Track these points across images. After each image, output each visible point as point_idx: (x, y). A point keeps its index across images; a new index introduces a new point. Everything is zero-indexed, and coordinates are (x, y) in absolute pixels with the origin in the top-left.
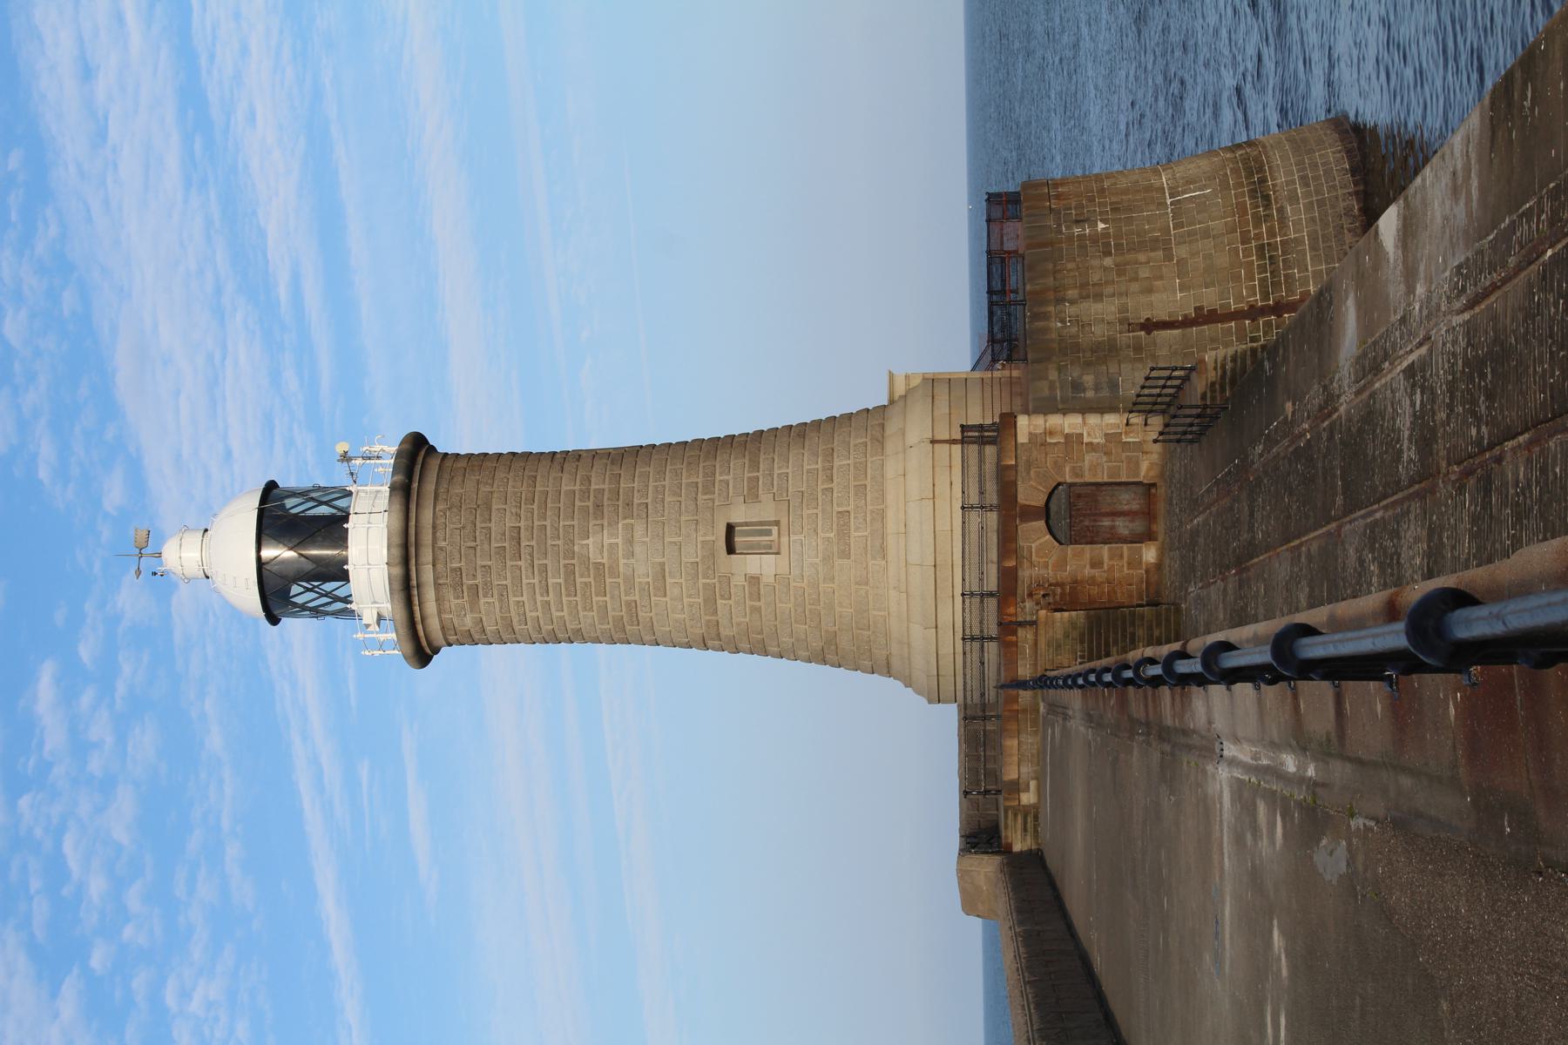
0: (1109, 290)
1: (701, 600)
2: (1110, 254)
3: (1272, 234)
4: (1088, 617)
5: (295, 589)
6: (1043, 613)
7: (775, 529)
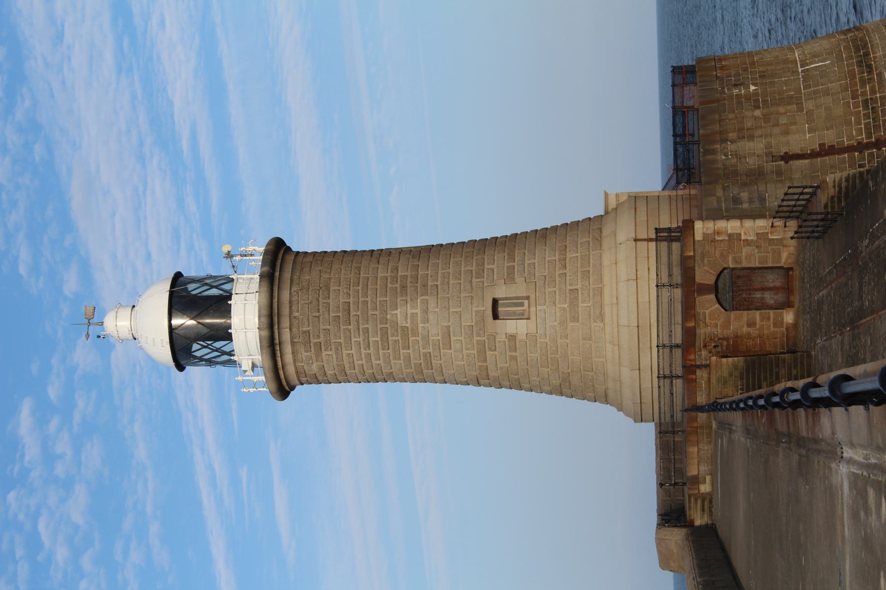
0: (758, 132)
1: (475, 352)
2: (758, 107)
3: (873, 91)
4: (746, 361)
5: (195, 347)
6: (714, 358)
7: (526, 302)
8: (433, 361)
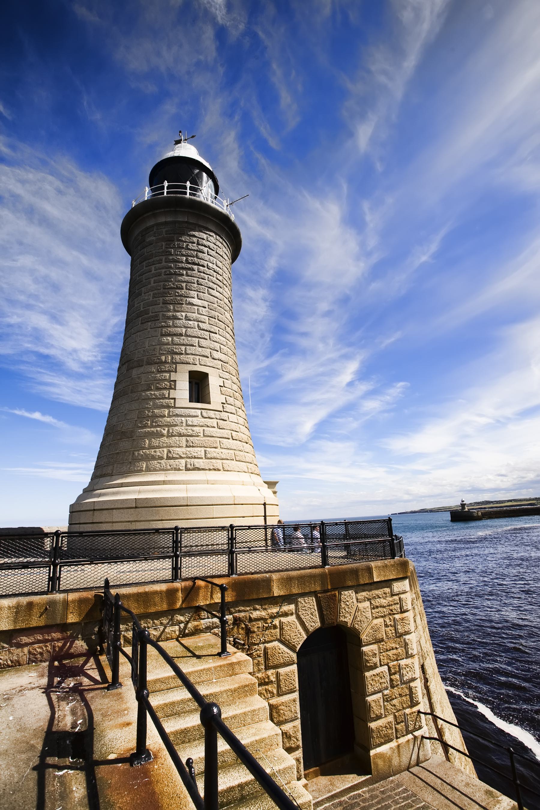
8: (149, 323)
